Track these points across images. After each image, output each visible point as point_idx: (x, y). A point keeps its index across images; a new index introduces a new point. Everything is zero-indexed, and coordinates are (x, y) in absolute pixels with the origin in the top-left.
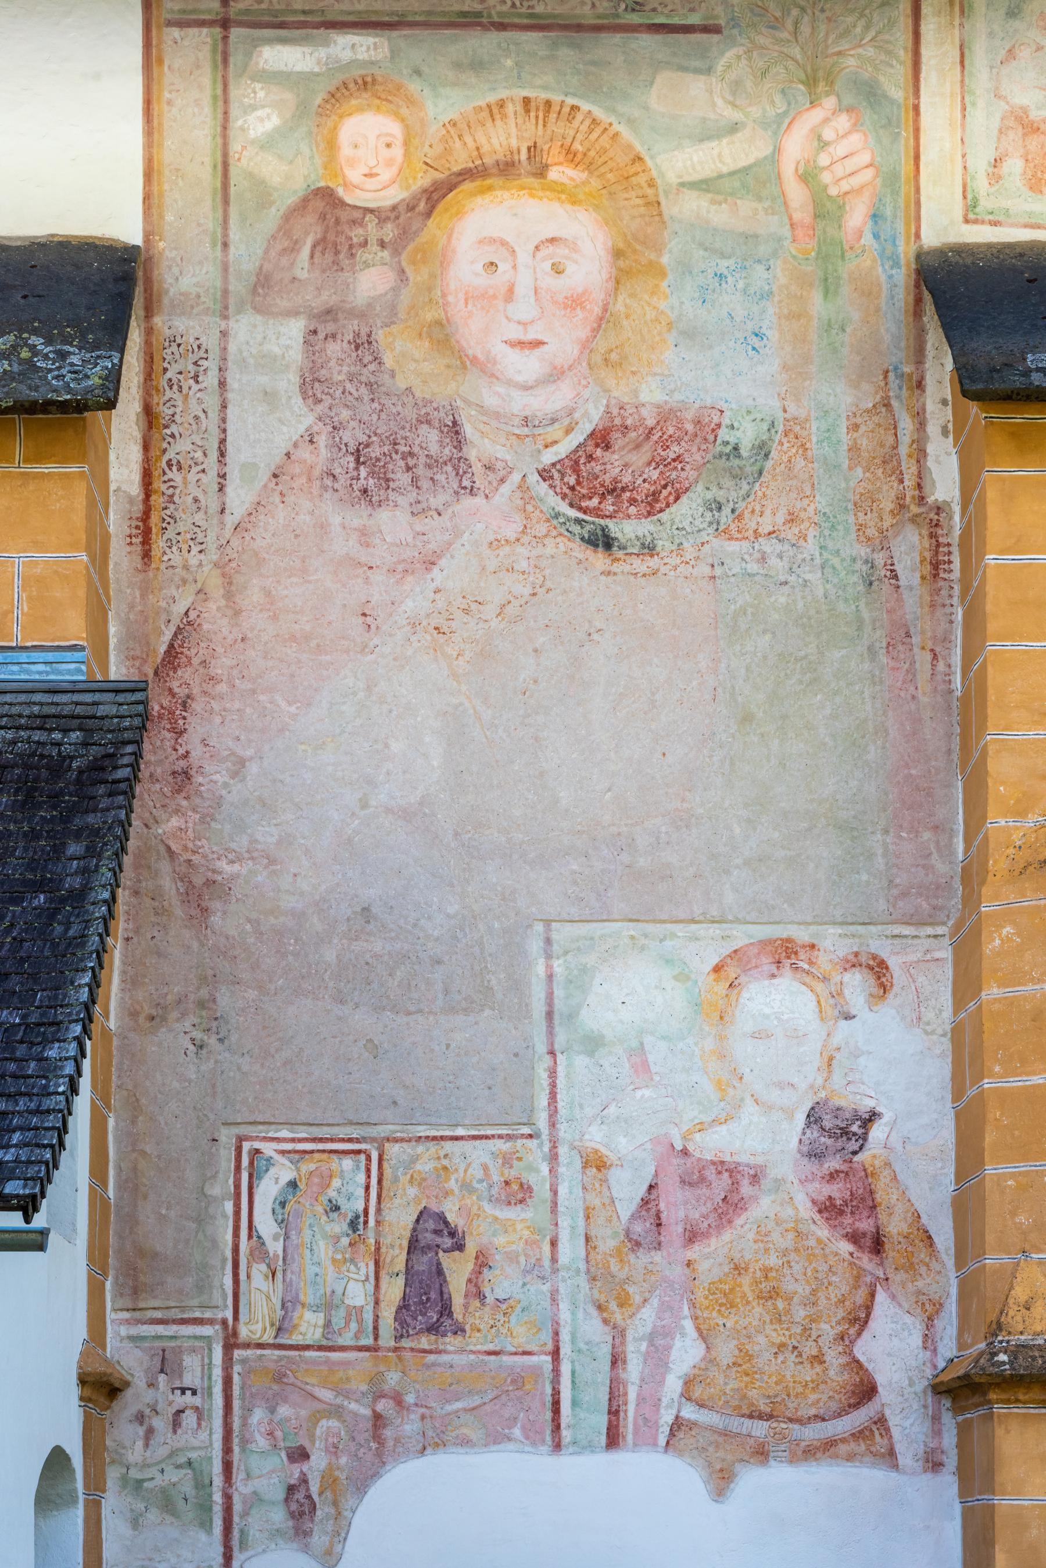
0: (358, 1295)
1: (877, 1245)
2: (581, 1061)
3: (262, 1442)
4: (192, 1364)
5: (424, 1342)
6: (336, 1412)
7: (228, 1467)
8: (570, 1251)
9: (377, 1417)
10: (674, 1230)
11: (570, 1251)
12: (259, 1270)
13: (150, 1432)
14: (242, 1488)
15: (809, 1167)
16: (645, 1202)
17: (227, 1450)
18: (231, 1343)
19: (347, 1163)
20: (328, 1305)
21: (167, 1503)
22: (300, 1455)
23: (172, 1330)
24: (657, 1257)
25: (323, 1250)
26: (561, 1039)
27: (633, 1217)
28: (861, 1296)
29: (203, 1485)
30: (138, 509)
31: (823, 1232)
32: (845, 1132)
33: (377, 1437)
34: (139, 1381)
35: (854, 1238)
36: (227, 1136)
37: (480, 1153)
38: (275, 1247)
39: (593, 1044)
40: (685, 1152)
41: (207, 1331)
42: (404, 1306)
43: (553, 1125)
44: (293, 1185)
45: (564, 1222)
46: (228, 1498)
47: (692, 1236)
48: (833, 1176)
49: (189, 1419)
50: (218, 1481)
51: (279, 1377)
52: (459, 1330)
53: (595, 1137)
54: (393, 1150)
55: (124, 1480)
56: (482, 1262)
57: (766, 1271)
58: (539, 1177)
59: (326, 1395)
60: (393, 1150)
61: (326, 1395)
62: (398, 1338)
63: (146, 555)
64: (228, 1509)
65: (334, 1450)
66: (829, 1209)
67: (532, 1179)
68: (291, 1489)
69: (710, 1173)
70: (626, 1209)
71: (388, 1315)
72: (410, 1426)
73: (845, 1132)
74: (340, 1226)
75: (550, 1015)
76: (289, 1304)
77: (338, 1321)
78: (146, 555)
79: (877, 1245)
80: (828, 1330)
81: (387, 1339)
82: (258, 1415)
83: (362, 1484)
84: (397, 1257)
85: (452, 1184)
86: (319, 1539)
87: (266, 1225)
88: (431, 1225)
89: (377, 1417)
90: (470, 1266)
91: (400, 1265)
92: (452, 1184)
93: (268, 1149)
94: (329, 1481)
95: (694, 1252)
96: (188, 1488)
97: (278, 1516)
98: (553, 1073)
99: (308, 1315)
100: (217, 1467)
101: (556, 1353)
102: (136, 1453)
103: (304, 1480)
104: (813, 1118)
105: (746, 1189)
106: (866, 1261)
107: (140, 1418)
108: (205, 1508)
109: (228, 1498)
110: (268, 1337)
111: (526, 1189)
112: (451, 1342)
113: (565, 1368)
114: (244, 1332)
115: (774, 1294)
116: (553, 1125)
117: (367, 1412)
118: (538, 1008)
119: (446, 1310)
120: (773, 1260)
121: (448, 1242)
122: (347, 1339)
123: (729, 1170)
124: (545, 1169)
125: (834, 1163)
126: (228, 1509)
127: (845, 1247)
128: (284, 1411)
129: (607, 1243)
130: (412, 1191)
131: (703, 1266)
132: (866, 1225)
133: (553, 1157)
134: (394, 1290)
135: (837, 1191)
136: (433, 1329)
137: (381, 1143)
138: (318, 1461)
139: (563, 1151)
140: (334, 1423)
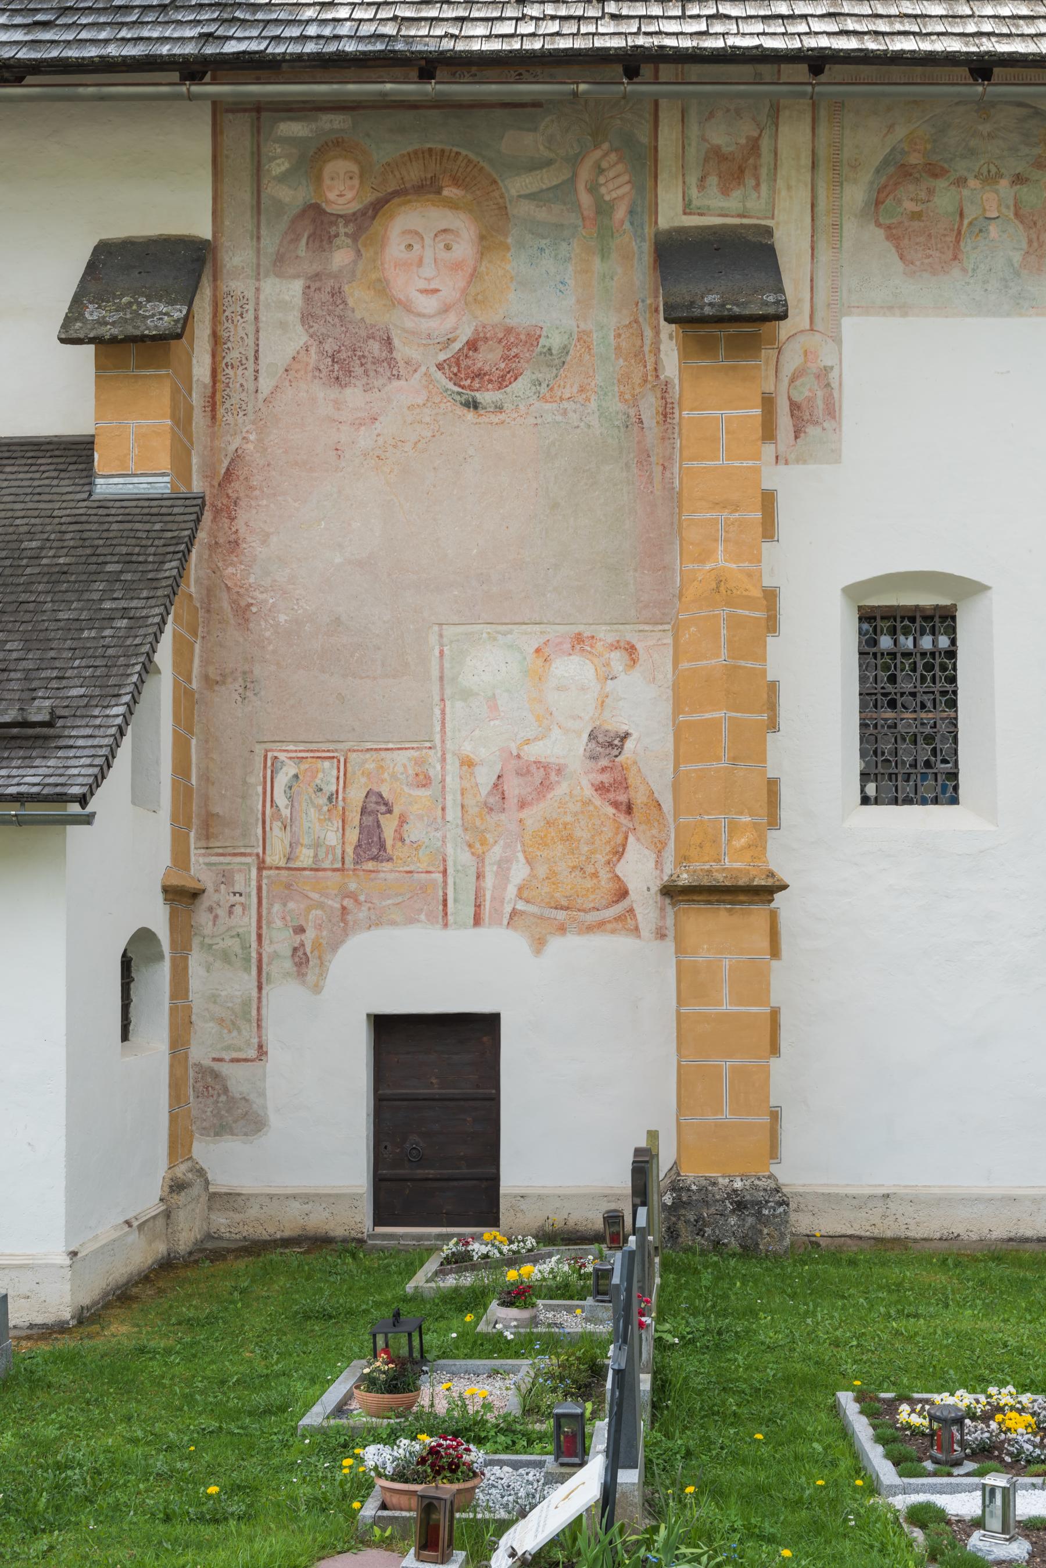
0: (332, 838)
1: (629, 809)
2: (459, 704)
3: (279, 923)
4: (239, 878)
5: (370, 865)
6: (321, 906)
7: (259, 937)
8: (453, 814)
9: (344, 908)
10: (512, 801)
11: (453, 814)
12: (277, 825)
13: (216, 917)
14: (267, 949)
15: (591, 764)
16: (496, 785)
17: (259, 927)
18: (261, 867)
19: (327, 764)
20: (317, 845)
21: (226, 957)
22: (300, 930)
23: (227, 859)
24: (503, 817)
26: (448, 692)
27: (490, 793)
28: (620, 839)
29: (246, 948)
30: (209, 392)
31: (598, 801)
32: (611, 745)
33: (343, 920)
34: (210, 888)
35: (615, 804)
36: (259, 749)
37: (402, 757)
38: (286, 812)
39: (466, 694)
40: (518, 756)
41: (248, 860)
42: (359, 846)
43: (443, 742)
44: (296, 776)
45: (449, 797)
46: (260, 955)
47: (522, 805)
48: (603, 770)
49: (238, 910)
50: (254, 945)
51: (288, 886)
52: (390, 859)
53: (467, 748)
54: (352, 756)
55: (202, 944)
56: (403, 820)
57: (565, 825)
58: (435, 770)
59: (315, 896)
60: (352, 756)
61: (315, 896)
63: (214, 417)
64: (260, 961)
65: (319, 927)
66: (601, 788)
67: (431, 773)
68: (295, 950)
69: (533, 769)
70: (484, 791)
71: (350, 850)
72: (362, 914)
73: (611, 745)
74: (322, 800)
75: (441, 678)
77: (321, 855)
78: (214, 417)
79: (629, 809)
80: (601, 858)
81: (349, 864)
82: (277, 907)
83: (335, 946)
84: (354, 817)
85: (386, 776)
86: (311, 978)
87: (281, 800)
88: (374, 799)
89: (344, 908)
90: (396, 822)
91: (356, 822)
92: (386, 776)
93: (282, 756)
94: (317, 945)
95: (524, 814)
96: (237, 949)
97: (288, 965)
98: (443, 712)
99: (305, 851)
100: (254, 937)
101: (445, 872)
102: (208, 929)
103: (303, 945)
104: (592, 736)
105: (553, 777)
106: (623, 819)
107: (211, 909)
108: (247, 960)
109: (260, 955)
110: (282, 864)
111: (427, 777)
112: (386, 866)
113: (450, 881)
114: (269, 860)
115: (569, 838)
116: (443, 742)
117: (338, 906)
118: (435, 673)
119: (382, 846)
120: (569, 819)
121: (383, 808)
122: (327, 864)
123: (544, 767)
124: (438, 767)
125: (604, 762)
126: (260, 961)
127: (611, 811)
128: (291, 905)
129: (473, 811)
130: (363, 780)
131: (529, 822)
132: (622, 798)
133: (443, 759)
134: (353, 836)
135: (606, 778)
136: (375, 858)
139: (448, 756)
140: (319, 912)
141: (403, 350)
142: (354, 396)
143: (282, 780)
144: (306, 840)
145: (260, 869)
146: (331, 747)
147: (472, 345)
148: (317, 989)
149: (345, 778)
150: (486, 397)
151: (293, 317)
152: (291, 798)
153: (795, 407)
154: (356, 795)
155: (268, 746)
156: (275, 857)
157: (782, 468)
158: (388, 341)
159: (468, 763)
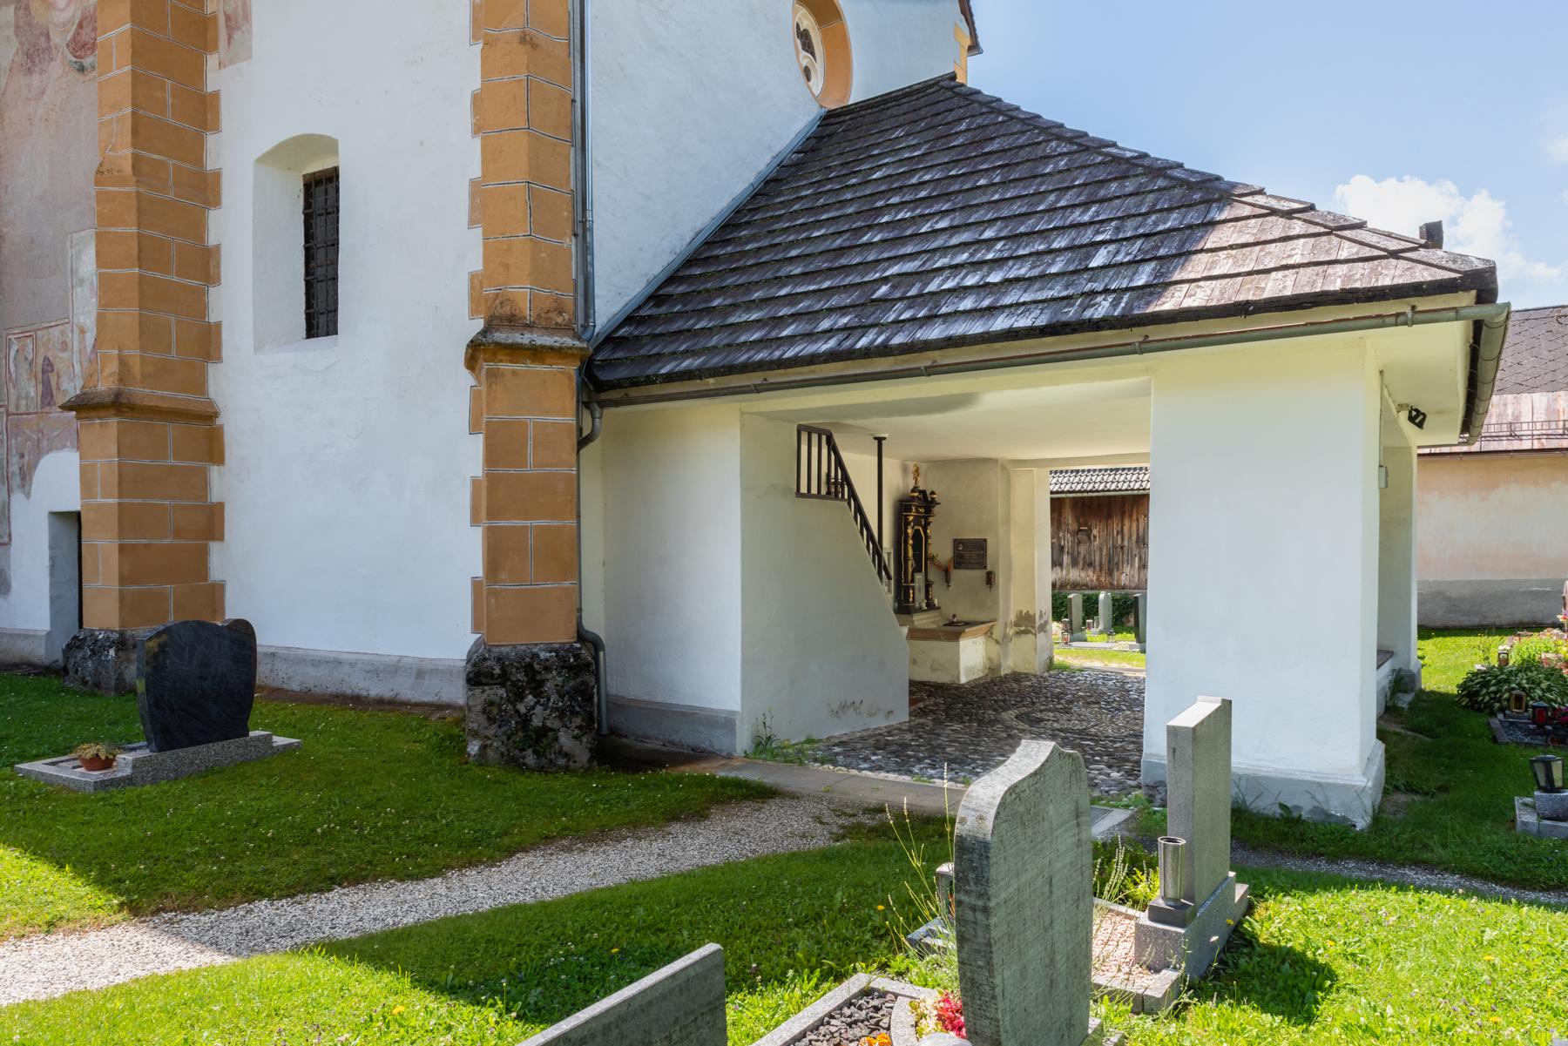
3: (14, 452)
14: (11, 469)
19: (29, 340)
20: (27, 396)
25: (24, 374)
62: (42, 408)
67: (68, 340)
68: (20, 469)
71: (39, 399)
76: (19, 397)
82: (13, 441)
84: (40, 375)
122: (31, 411)
128: (19, 439)
137: (35, 331)
138: (26, 458)
141: (56, 39)
142: (35, 79)
143: (13, 353)
144: (23, 395)
145: (7, 415)
146: (29, 328)
147: (80, 26)
148: (28, 495)
149: (36, 349)
150: (87, 61)
151: (11, 32)
152: (16, 366)
153: (228, 18)
154: (40, 360)
155: (9, 331)
156: (12, 409)
157: (223, 71)
158: (48, 36)
159: (82, 331)
